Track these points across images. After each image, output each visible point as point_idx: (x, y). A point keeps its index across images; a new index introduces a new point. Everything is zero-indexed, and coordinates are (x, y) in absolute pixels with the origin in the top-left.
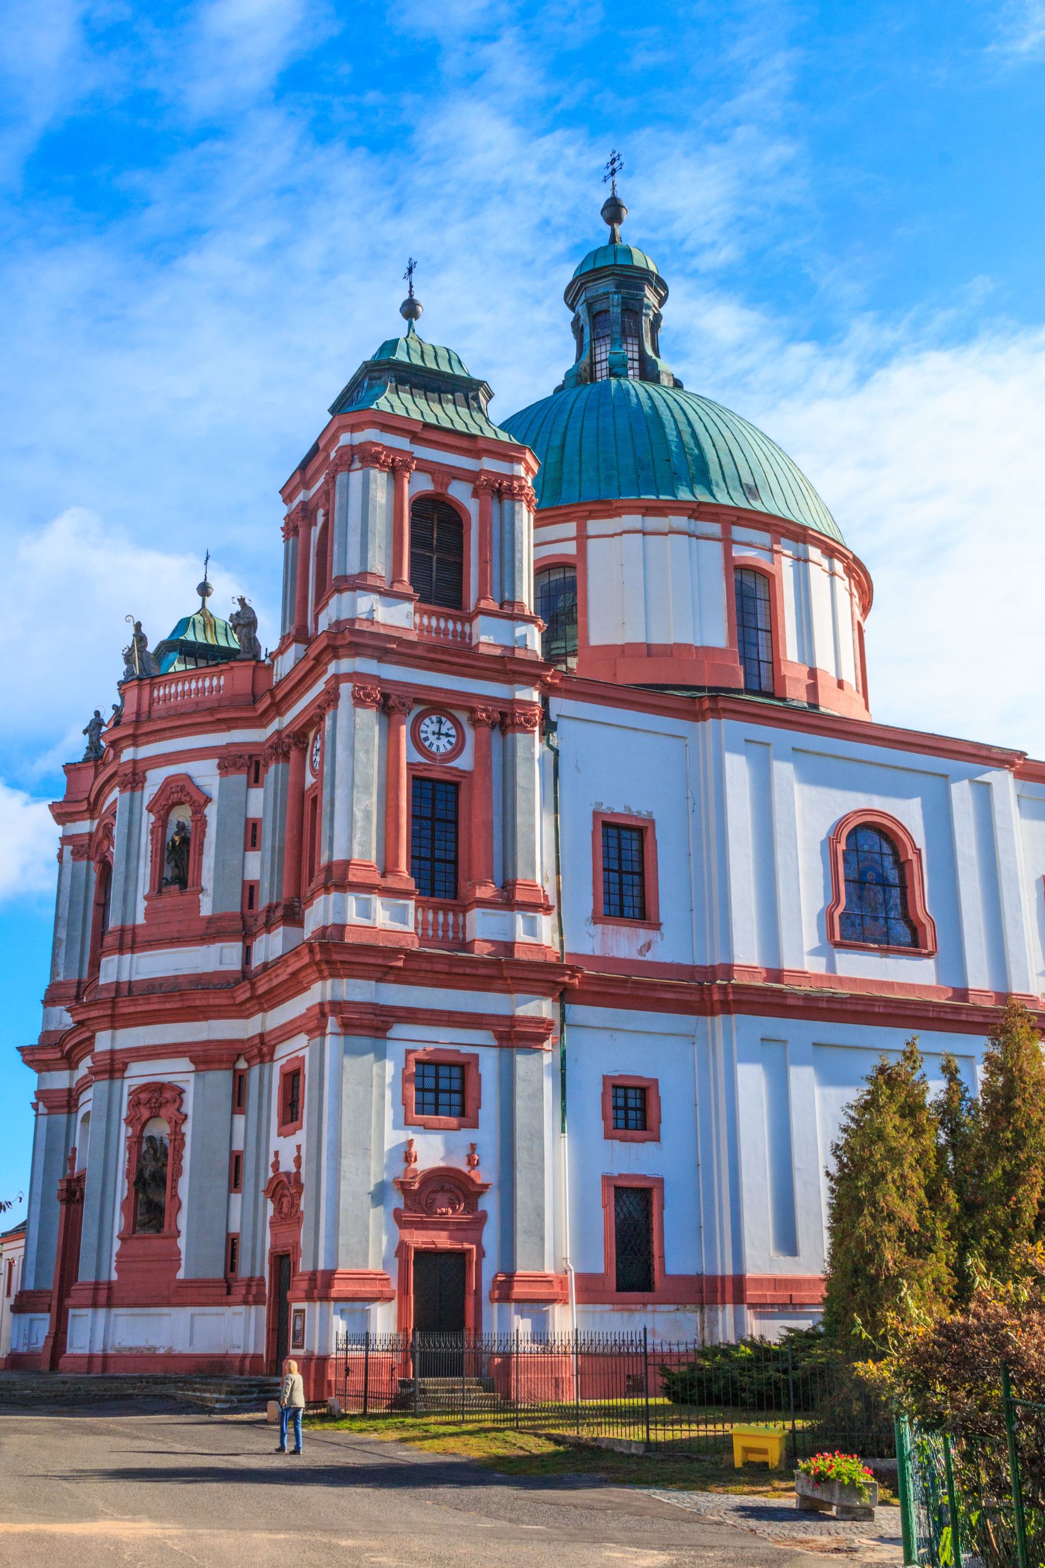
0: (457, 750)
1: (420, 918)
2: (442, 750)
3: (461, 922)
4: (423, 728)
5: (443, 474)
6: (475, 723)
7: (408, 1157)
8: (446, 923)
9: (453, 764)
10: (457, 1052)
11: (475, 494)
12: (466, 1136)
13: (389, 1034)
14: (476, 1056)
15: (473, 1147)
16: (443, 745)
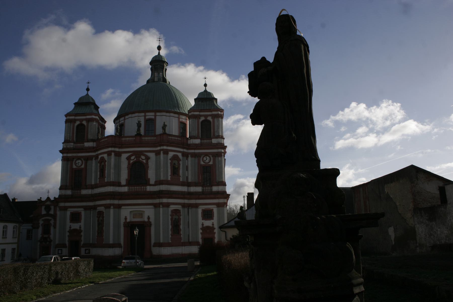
0: (210, 161)
1: (203, 188)
2: (207, 162)
3: (212, 188)
4: (204, 159)
5: (206, 116)
6: (212, 156)
7: (203, 225)
8: (209, 189)
9: (209, 164)
10: (210, 209)
11: (212, 118)
12: (212, 221)
13: (199, 207)
14: (213, 209)
15: (213, 223)
16: (207, 161)
